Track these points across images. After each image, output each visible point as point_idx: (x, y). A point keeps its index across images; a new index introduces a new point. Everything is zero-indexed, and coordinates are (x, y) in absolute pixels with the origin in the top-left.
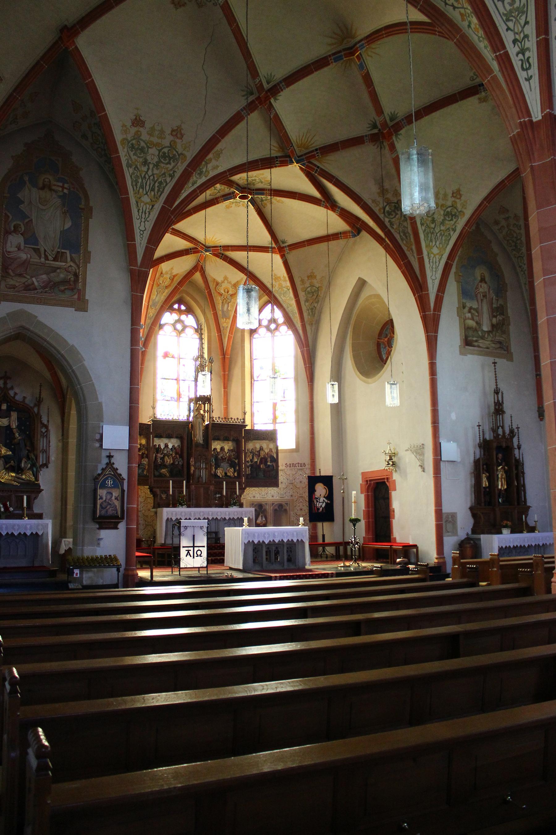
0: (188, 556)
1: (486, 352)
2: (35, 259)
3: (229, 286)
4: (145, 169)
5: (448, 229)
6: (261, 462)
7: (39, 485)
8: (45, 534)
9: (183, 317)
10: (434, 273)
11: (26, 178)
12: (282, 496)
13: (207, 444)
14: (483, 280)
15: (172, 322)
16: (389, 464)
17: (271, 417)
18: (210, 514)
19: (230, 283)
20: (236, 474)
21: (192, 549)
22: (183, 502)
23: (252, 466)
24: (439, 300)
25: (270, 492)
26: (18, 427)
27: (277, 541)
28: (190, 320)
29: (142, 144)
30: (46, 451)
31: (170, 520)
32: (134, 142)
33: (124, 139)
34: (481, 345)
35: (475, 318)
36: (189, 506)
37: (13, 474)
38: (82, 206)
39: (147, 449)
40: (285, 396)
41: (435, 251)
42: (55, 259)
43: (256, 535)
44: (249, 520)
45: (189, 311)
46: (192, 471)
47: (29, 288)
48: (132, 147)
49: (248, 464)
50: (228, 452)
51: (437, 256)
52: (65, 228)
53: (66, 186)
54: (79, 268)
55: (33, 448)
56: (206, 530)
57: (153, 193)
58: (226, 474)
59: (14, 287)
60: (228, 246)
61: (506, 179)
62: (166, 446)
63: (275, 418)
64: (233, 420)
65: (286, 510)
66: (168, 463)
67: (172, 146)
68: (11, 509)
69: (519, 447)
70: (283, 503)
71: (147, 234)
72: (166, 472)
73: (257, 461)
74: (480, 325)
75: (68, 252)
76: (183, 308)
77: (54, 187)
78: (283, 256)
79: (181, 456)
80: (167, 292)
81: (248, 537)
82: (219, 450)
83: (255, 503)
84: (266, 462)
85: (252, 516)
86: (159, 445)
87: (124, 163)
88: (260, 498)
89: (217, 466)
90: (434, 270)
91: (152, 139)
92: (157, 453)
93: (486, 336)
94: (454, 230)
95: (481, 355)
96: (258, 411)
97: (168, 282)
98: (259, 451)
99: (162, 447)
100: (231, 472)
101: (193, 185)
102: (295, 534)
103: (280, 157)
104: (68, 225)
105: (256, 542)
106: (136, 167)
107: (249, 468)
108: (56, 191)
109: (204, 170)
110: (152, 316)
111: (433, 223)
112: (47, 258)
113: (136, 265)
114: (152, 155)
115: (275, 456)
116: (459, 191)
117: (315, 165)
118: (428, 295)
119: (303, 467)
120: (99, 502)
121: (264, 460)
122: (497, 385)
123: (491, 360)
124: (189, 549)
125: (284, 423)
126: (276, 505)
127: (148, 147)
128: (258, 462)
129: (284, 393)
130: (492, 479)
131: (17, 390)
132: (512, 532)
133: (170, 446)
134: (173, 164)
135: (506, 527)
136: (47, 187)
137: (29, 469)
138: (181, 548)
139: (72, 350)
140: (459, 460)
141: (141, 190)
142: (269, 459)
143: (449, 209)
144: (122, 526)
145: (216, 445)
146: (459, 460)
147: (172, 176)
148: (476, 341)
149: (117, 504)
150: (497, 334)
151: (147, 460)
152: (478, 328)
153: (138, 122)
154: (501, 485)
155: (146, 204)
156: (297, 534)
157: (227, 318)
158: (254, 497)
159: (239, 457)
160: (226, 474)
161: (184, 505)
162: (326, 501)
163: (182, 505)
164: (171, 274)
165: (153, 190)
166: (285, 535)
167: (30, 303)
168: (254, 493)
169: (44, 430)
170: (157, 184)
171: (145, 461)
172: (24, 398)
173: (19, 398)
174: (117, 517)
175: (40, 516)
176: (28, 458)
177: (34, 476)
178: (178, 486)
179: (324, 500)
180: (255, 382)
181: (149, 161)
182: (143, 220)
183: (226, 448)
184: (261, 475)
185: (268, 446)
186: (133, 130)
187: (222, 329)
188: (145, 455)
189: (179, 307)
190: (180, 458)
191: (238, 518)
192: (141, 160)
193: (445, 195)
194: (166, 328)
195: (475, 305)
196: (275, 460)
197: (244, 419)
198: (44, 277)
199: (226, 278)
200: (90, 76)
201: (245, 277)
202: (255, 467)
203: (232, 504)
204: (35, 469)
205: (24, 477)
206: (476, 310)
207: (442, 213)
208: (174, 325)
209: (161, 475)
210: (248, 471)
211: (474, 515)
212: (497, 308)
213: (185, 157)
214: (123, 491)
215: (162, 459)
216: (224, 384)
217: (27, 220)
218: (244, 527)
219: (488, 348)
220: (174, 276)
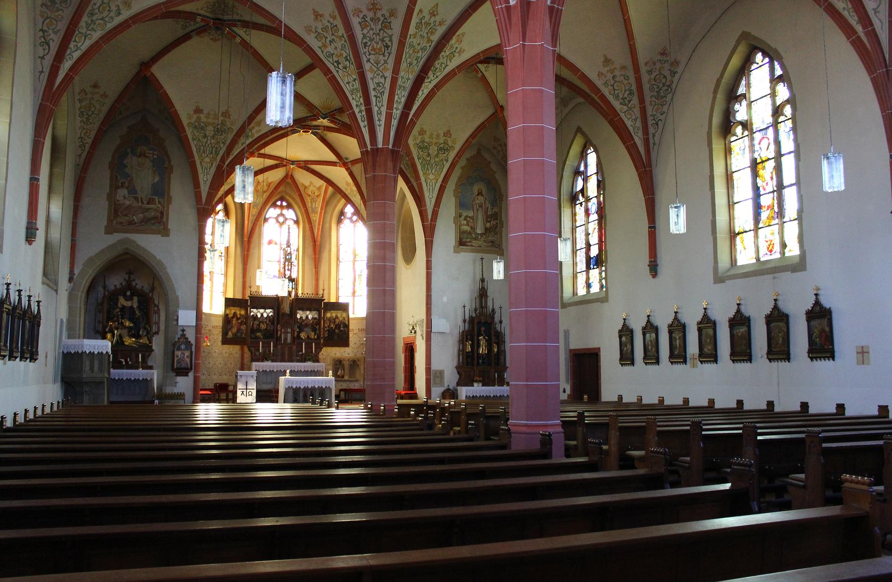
1: (479, 250)
2: (135, 204)
3: (315, 189)
4: (205, 140)
5: (442, 160)
7: (151, 346)
8: (152, 380)
9: (285, 212)
10: (431, 193)
11: (129, 150)
13: (293, 314)
14: (480, 193)
15: (276, 216)
16: (411, 332)
17: (352, 291)
19: (315, 186)
20: (316, 337)
23: (328, 330)
24: (435, 213)
26: (138, 307)
27: (310, 387)
28: (290, 214)
29: (202, 124)
30: (158, 323)
32: (196, 124)
33: (189, 123)
34: (474, 244)
35: (470, 223)
36: (273, 361)
37: (134, 340)
38: (166, 166)
39: (245, 318)
41: (431, 177)
42: (148, 203)
43: (295, 382)
45: (289, 206)
46: (279, 335)
47: (131, 223)
48: (196, 127)
49: (326, 329)
51: (433, 181)
52: (155, 181)
53: (155, 153)
54: (163, 207)
55: (148, 322)
56: (255, 378)
57: (211, 156)
58: (308, 336)
59: (121, 223)
60: (308, 161)
61: (485, 121)
62: (262, 315)
63: (354, 292)
65: (358, 365)
67: (223, 123)
68: (130, 363)
69: (501, 322)
71: (208, 183)
74: (474, 229)
75: (157, 198)
76: (284, 204)
77: (147, 155)
78: (347, 169)
79: (273, 323)
80: (265, 196)
82: (304, 318)
87: (190, 137)
90: (431, 191)
91: (208, 120)
93: (479, 237)
94: (447, 161)
95: (473, 252)
97: (265, 188)
99: (259, 316)
100: (312, 335)
101: (242, 145)
103: (310, 116)
104: (157, 179)
106: (199, 139)
108: (148, 157)
109: (250, 134)
111: (428, 157)
112: (142, 203)
113: (201, 204)
114: (210, 131)
116: (449, 132)
117: (338, 120)
118: (426, 210)
120: (176, 359)
121: (338, 326)
122: (483, 276)
123: (480, 255)
127: (206, 126)
130: (476, 345)
131: (137, 282)
132: (482, 386)
133: (265, 315)
134: (224, 135)
135: (476, 381)
136: (143, 155)
137: (145, 335)
138: (238, 390)
139: (159, 262)
140: (448, 332)
141: (203, 155)
142: (342, 326)
143: (442, 146)
144: (191, 374)
145: (300, 315)
146: (448, 332)
147: (224, 143)
148: (470, 242)
149: (188, 360)
150: (490, 235)
151: (245, 326)
152: (472, 231)
153: (198, 111)
154: (482, 350)
155: (207, 163)
157: (316, 213)
159: (319, 324)
160: (308, 336)
163: (268, 360)
164: (267, 182)
165: (212, 153)
167: (132, 233)
169: (156, 309)
170: (214, 149)
171: (243, 327)
172: (143, 287)
173: (138, 287)
174: (187, 369)
175: (151, 368)
176: (145, 328)
177: (148, 339)
178: (267, 346)
181: (208, 134)
182: (205, 174)
183: (310, 317)
185: (342, 315)
186: (195, 116)
187: (312, 222)
189: (281, 204)
192: (202, 135)
193: (438, 136)
194: (270, 221)
195: (471, 214)
197: (323, 294)
198: (141, 215)
199: (311, 183)
200: (162, 88)
201: (325, 184)
202: (331, 332)
204: (149, 336)
205: (141, 341)
206: (472, 218)
207: (436, 148)
208: (277, 219)
209: (256, 338)
210: (326, 335)
211: (459, 373)
212: (492, 216)
213: (233, 129)
214: (192, 352)
215: (259, 325)
216: (315, 265)
217: (129, 179)
218: (286, 377)
219: (480, 246)
220: (270, 183)
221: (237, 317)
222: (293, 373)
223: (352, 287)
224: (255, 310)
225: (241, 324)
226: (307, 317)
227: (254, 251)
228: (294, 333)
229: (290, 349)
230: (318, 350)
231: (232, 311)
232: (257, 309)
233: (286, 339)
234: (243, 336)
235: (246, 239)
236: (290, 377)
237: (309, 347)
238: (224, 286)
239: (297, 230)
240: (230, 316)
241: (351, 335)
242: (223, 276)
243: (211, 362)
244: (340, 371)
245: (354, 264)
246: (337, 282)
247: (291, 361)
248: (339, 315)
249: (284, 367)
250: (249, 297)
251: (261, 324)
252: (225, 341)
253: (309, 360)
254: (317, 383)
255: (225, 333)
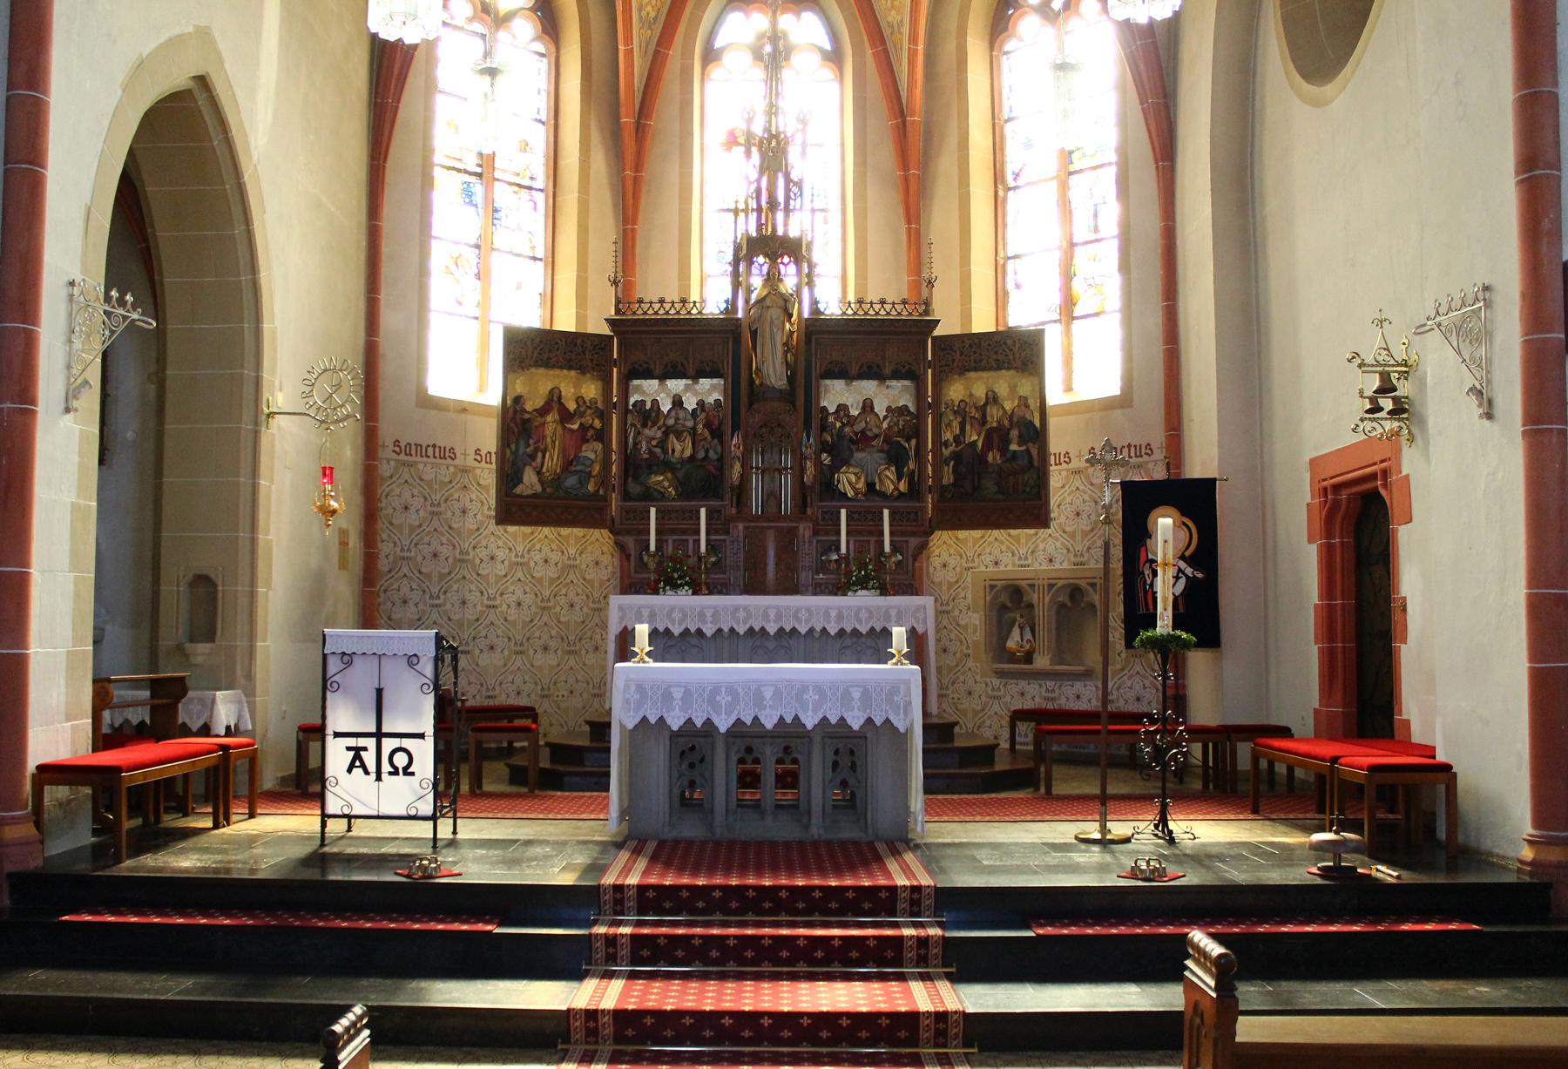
0: (358, 771)
6: (988, 444)
12: (1079, 559)
17: (1056, 299)
18: (709, 619)
20: (903, 486)
21: (371, 743)
22: (680, 577)
23: (956, 456)
25: (1041, 546)
28: (807, 30)
31: (817, 635)
40: (1100, 228)
43: (678, 694)
44: (917, 641)
49: (946, 452)
50: (885, 417)
56: (429, 670)
62: (677, 402)
64: (888, 307)
66: (677, 454)
70: (1083, 583)
72: (666, 484)
73: (976, 441)
79: (717, 433)
81: (639, 704)
82: (854, 412)
83: (999, 583)
84: (1006, 441)
85: (925, 621)
86: (655, 402)
88: (1014, 565)
89: (840, 462)
92: (644, 425)
96: (1018, 286)
98: (986, 404)
99: (666, 407)
100: (889, 481)
102: (856, 694)
105: (675, 723)
107: (948, 465)
110: (653, 14)
115: (1037, 423)
119: (1146, 458)
121: (997, 437)
124: (362, 742)
125: (1097, 315)
126: (1064, 586)
128: (980, 444)
129: (1096, 216)
133: (690, 403)
138: (330, 740)
142: (1014, 433)
145: (837, 395)
151: (598, 446)
156: (866, 696)
158: (996, 563)
159: (917, 432)
160: (870, 486)
161: (682, 585)
162: (1189, 571)
163: (675, 587)
166: (811, 696)
168: (995, 552)
178: (677, 525)
179: (1180, 570)
180: (1011, 193)
184: (989, 485)
185: (1013, 388)
187: (886, 32)
188: (591, 433)
190: (713, 438)
191: (872, 629)
194: (727, 58)
196: (1036, 434)
202: (968, 463)
203: (854, 584)
209: (649, 496)
210: (948, 478)
215: (662, 444)
221: (563, 411)
222: (667, 644)
223: (1056, 282)
224: (653, 384)
225: (583, 435)
226: (868, 406)
227: (660, 166)
228: (803, 470)
229: (787, 543)
230: (914, 542)
231: (539, 385)
232: (663, 377)
233: (772, 496)
234: (591, 488)
235: (627, 120)
236: (652, 664)
237: (865, 523)
238: (542, 304)
239: (835, 86)
240: (529, 406)
241: (1055, 481)
242: (540, 265)
243: (473, 598)
244: (1016, 631)
245: (1064, 188)
246: (999, 271)
247: (794, 590)
248: (1002, 389)
249: (749, 615)
250: (611, 322)
251: (672, 437)
252: (512, 509)
253: (863, 584)
254: (811, 696)
255: (508, 477)
